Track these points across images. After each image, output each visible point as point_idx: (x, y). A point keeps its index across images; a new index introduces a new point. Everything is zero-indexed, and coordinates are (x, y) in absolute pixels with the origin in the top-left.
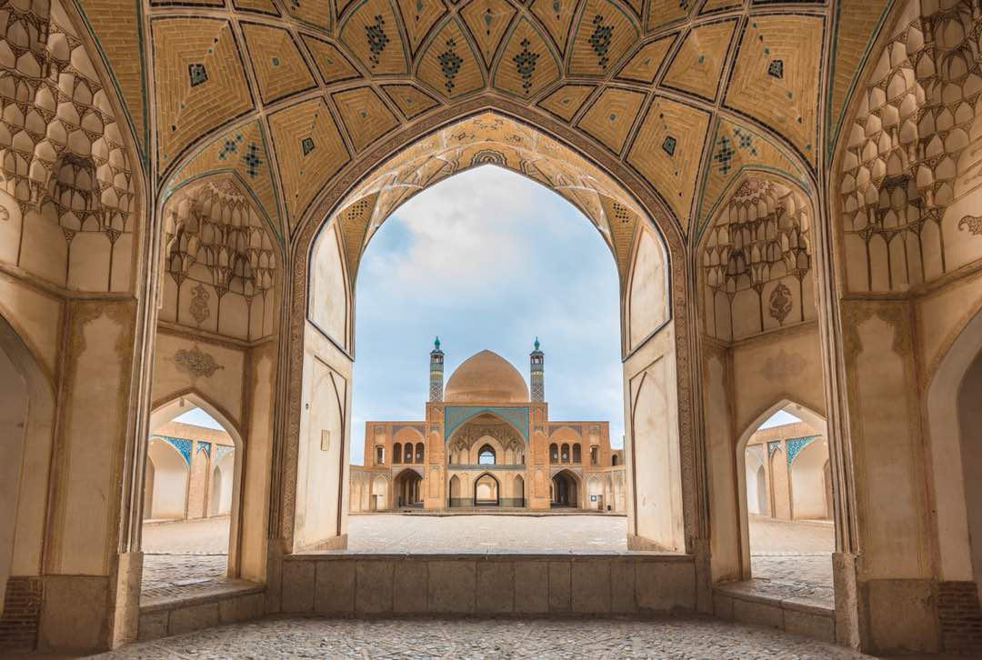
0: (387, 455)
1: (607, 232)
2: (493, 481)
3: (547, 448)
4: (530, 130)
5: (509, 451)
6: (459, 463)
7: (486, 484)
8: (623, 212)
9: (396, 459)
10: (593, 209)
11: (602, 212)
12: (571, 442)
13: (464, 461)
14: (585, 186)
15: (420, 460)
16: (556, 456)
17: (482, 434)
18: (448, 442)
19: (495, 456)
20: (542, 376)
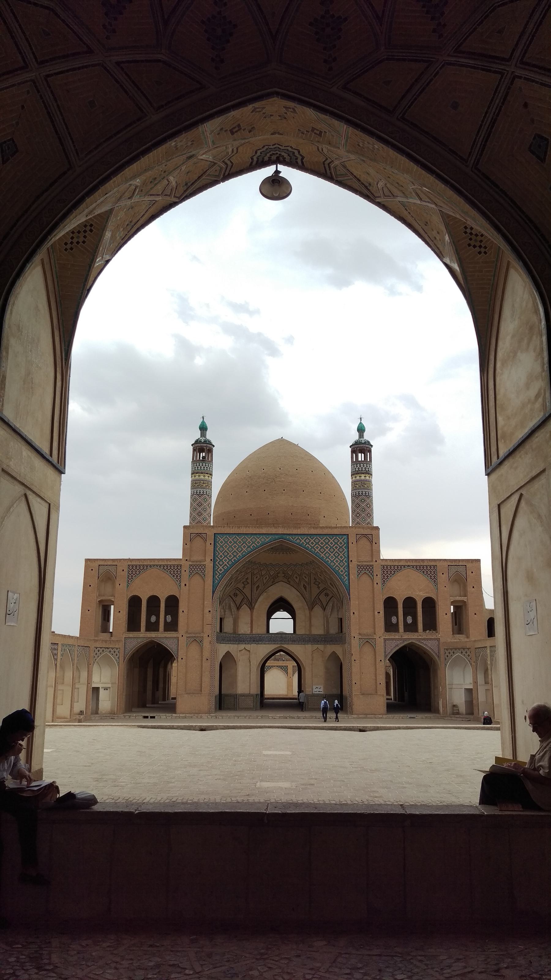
1: (456, 267)
2: (291, 664)
3: (380, 607)
4: (336, 123)
5: (318, 609)
6: (235, 632)
7: (281, 667)
8: (479, 238)
9: (133, 624)
10: (435, 233)
11: (447, 238)
12: (419, 596)
13: (244, 629)
14: (421, 199)
15: (172, 626)
16: (394, 620)
17: (274, 580)
18: (218, 594)
19: (294, 618)
20: (370, 482)
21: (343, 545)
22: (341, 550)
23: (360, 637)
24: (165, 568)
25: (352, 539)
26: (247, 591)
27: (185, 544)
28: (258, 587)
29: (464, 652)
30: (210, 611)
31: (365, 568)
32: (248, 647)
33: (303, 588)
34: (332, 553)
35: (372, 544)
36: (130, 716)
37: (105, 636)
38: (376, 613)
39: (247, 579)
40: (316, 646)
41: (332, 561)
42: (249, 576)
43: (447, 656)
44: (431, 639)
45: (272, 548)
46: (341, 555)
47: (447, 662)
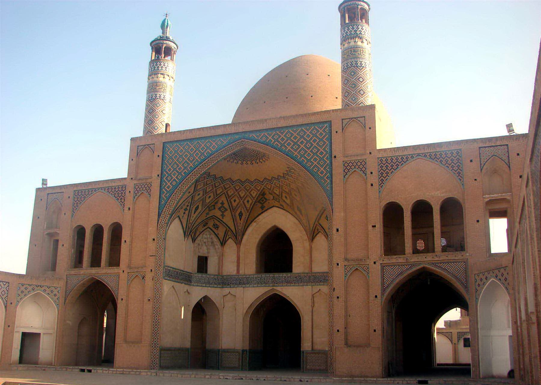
0: (66, 252)
5: (320, 239)
12: (435, 197)
13: (230, 269)
15: (114, 262)
21: (324, 137)
22: (321, 143)
23: (346, 263)
24: (110, 190)
25: (337, 126)
26: (228, 219)
27: (131, 159)
28: (241, 215)
29: (499, 276)
30: (154, 240)
31: (355, 164)
32: (233, 291)
33: (298, 213)
34: (308, 149)
35: (364, 131)
36: (67, 369)
37: (50, 273)
38: (370, 227)
39: (223, 203)
40: (316, 288)
41: (309, 161)
42: (223, 199)
43: (479, 285)
44: (455, 261)
45: (234, 154)
46: (322, 150)
47: (479, 295)
